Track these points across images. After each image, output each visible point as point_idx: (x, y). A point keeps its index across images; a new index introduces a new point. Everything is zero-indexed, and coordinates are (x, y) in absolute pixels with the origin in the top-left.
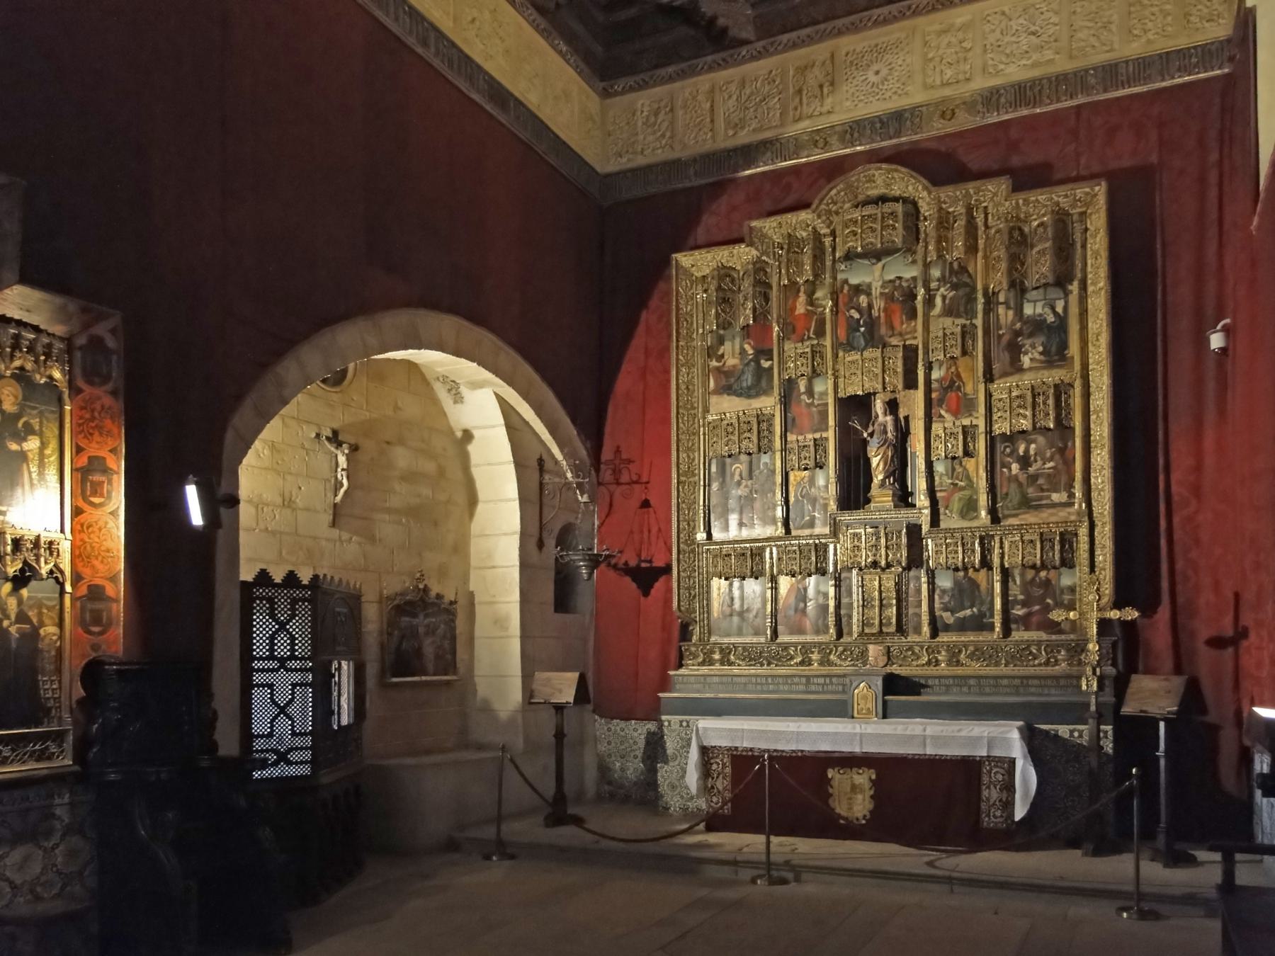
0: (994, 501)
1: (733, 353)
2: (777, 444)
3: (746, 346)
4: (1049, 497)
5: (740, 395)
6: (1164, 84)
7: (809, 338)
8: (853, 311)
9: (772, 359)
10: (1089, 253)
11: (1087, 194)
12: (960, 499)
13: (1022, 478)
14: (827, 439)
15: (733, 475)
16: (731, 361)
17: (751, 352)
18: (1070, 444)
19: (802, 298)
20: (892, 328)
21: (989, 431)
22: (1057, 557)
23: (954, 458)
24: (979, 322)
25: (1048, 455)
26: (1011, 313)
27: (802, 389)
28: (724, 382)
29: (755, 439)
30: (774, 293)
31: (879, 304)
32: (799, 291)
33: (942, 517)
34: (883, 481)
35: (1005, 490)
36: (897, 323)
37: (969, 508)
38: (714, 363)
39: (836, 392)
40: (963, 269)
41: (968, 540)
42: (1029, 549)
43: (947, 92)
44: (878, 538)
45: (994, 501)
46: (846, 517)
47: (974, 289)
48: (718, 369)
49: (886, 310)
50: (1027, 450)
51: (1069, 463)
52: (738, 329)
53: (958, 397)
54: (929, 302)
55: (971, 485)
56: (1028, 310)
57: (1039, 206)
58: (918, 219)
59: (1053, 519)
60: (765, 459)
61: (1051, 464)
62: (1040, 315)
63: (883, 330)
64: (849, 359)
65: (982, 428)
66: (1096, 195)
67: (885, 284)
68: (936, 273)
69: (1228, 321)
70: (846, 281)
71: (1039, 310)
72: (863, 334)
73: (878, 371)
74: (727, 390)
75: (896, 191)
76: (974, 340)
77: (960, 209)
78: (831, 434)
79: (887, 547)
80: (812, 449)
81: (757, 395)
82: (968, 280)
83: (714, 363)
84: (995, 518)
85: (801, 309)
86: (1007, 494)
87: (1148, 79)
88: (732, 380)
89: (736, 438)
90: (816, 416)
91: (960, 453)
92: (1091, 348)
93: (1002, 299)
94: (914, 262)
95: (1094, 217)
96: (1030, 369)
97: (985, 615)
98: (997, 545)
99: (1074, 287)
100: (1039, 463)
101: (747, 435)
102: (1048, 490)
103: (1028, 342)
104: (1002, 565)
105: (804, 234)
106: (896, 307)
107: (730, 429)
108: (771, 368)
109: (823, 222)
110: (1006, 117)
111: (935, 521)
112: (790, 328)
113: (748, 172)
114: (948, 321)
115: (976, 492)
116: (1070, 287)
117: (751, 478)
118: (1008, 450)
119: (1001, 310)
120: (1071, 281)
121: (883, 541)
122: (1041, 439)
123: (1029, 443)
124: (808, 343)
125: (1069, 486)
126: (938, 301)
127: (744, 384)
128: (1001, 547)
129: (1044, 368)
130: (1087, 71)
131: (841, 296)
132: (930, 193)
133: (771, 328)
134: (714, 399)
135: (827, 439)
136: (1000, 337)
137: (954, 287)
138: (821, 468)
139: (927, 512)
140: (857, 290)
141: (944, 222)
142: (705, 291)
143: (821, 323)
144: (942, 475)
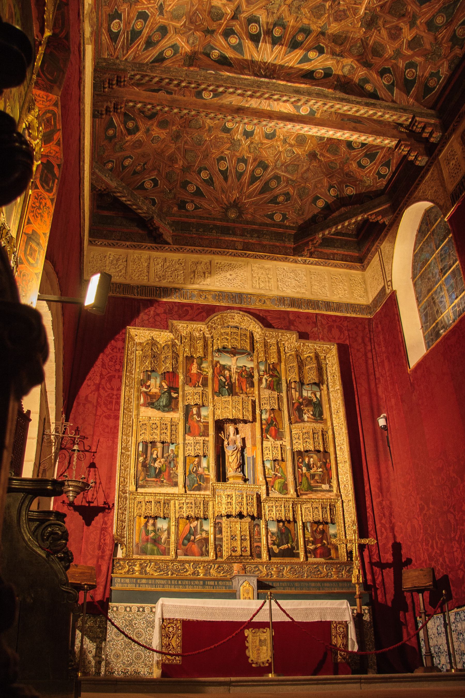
0: (296, 487)
1: (155, 385)
2: (181, 441)
3: (163, 384)
4: (321, 486)
5: (159, 409)
6: (348, 315)
7: (198, 386)
8: (222, 377)
9: (178, 393)
10: (329, 374)
11: (328, 348)
12: (279, 483)
13: (308, 475)
14: (208, 441)
15: (152, 454)
16: (154, 390)
17: (166, 387)
18: (328, 461)
19: (195, 366)
20: (242, 390)
21: (292, 449)
22: (329, 518)
23: (275, 461)
24: (284, 394)
25: (319, 465)
26: (297, 393)
27: (195, 412)
28: (149, 401)
29: (169, 434)
30: (181, 359)
31: (235, 377)
32: (193, 362)
33: (270, 492)
34: (236, 469)
35: (300, 481)
36: (244, 388)
37: (284, 488)
38: (144, 389)
39: (214, 417)
40: (274, 369)
41: (287, 504)
42: (316, 512)
43: (262, 292)
44: (242, 498)
45: (296, 487)
46: (220, 485)
47: (280, 379)
48: (146, 392)
49: (238, 380)
50: (309, 461)
51: (329, 470)
52: (160, 373)
53: (275, 430)
54: (260, 381)
55: (284, 477)
56: (305, 394)
57: (309, 348)
58: (253, 341)
59: (323, 497)
60: (172, 447)
61: (321, 470)
62: (310, 397)
63: (237, 390)
64: (225, 399)
65: (288, 447)
66: (331, 350)
67: (238, 368)
68: (262, 368)
69: (385, 415)
70: (218, 362)
71: (309, 395)
72: (227, 389)
73: (240, 408)
74: (151, 404)
75: (243, 326)
76: (282, 403)
77: (273, 341)
78: (211, 439)
79: (247, 504)
80: (202, 444)
81: (168, 411)
82: (277, 374)
83: (144, 389)
84: (298, 496)
85: (194, 370)
86: (301, 483)
87: (341, 311)
88: (154, 400)
89: (158, 432)
90: (202, 428)
91: (280, 458)
92: (334, 416)
93: (293, 386)
94: (252, 360)
95: (330, 358)
96: (308, 421)
97: (294, 548)
98: (300, 509)
99: (324, 387)
100: (315, 468)
101: (165, 431)
102: (320, 483)
103: (306, 409)
104: (302, 520)
105: (198, 335)
106: (244, 380)
107: (154, 426)
108: (177, 398)
109: (209, 331)
110: (289, 309)
111: (268, 494)
112: (188, 379)
113: (165, 300)
114: (270, 391)
115: (286, 480)
116: (322, 388)
117: (163, 457)
118: (300, 460)
119: (293, 391)
120: (323, 384)
121: (245, 499)
122: (315, 456)
123: (310, 457)
124: (198, 388)
125: (330, 482)
126: (264, 381)
127: (161, 404)
128: (301, 511)
129: (314, 422)
130: (319, 301)
131: (216, 368)
132: (262, 330)
133: (178, 377)
134: (143, 409)
135: (208, 441)
136: (293, 404)
137: (271, 376)
138: (205, 456)
139: (264, 488)
140: (224, 367)
141: (266, 345)
142: (142, 350)
143: (206, 379)
144: (269, 469)
